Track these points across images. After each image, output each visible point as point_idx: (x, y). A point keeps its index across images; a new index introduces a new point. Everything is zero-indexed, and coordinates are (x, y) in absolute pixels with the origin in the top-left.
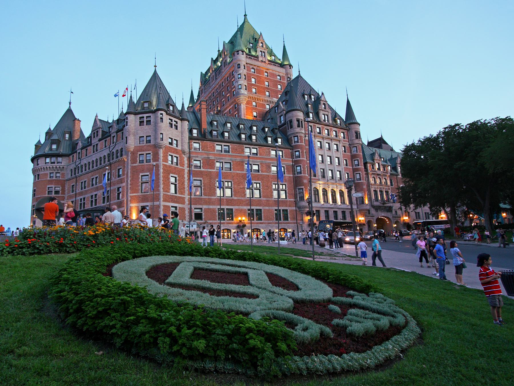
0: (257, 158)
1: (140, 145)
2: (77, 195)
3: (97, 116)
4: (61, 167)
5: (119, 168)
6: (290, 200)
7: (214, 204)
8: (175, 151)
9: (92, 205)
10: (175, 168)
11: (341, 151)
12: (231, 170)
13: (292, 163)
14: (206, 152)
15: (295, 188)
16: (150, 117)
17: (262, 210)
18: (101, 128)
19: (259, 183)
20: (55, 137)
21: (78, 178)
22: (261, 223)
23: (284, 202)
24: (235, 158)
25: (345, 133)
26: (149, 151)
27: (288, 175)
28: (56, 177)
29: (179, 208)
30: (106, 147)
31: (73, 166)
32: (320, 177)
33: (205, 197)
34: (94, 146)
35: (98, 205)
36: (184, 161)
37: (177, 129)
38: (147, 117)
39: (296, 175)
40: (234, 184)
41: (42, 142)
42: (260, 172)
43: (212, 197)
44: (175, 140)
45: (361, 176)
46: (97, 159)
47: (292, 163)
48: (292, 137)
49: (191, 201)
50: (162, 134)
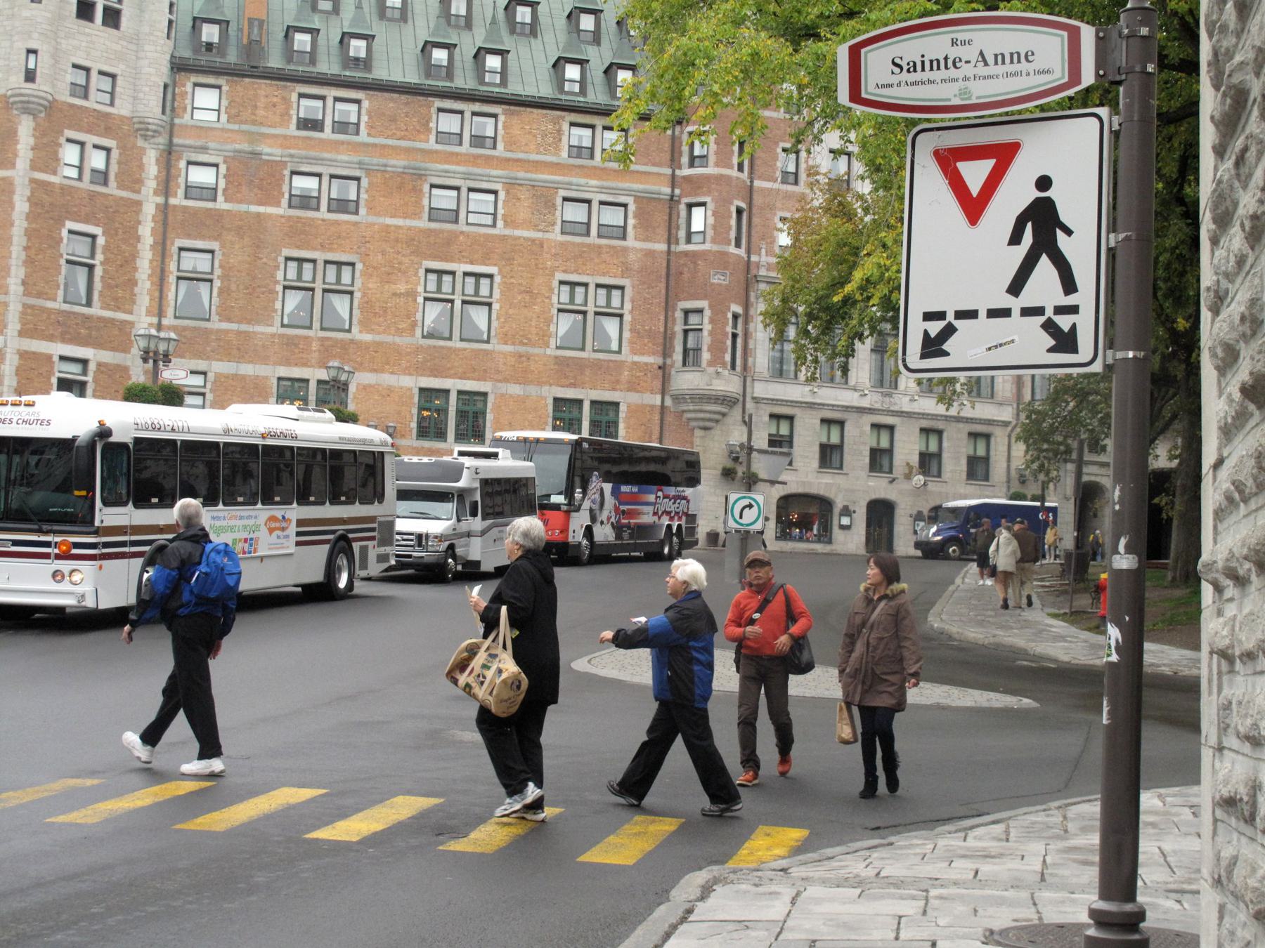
6: (636, 358)
7: (264, 360)
8: (103, 123)
10: (93, 196)
12: (357, 213)
14: (245, 127)
15: (668, 307)
17: (491, 399)
19: (491, 276)
23: (606, 371)
24: (382, 156)
27: (639, 245)
29: (99, 365)
33: (225, 326)
36: (141, 167)
39: (682, 247)
42: (500, 223)
43: (259, 329)
44: (101, 73)
47: (668, 190)
50: (35, 52)
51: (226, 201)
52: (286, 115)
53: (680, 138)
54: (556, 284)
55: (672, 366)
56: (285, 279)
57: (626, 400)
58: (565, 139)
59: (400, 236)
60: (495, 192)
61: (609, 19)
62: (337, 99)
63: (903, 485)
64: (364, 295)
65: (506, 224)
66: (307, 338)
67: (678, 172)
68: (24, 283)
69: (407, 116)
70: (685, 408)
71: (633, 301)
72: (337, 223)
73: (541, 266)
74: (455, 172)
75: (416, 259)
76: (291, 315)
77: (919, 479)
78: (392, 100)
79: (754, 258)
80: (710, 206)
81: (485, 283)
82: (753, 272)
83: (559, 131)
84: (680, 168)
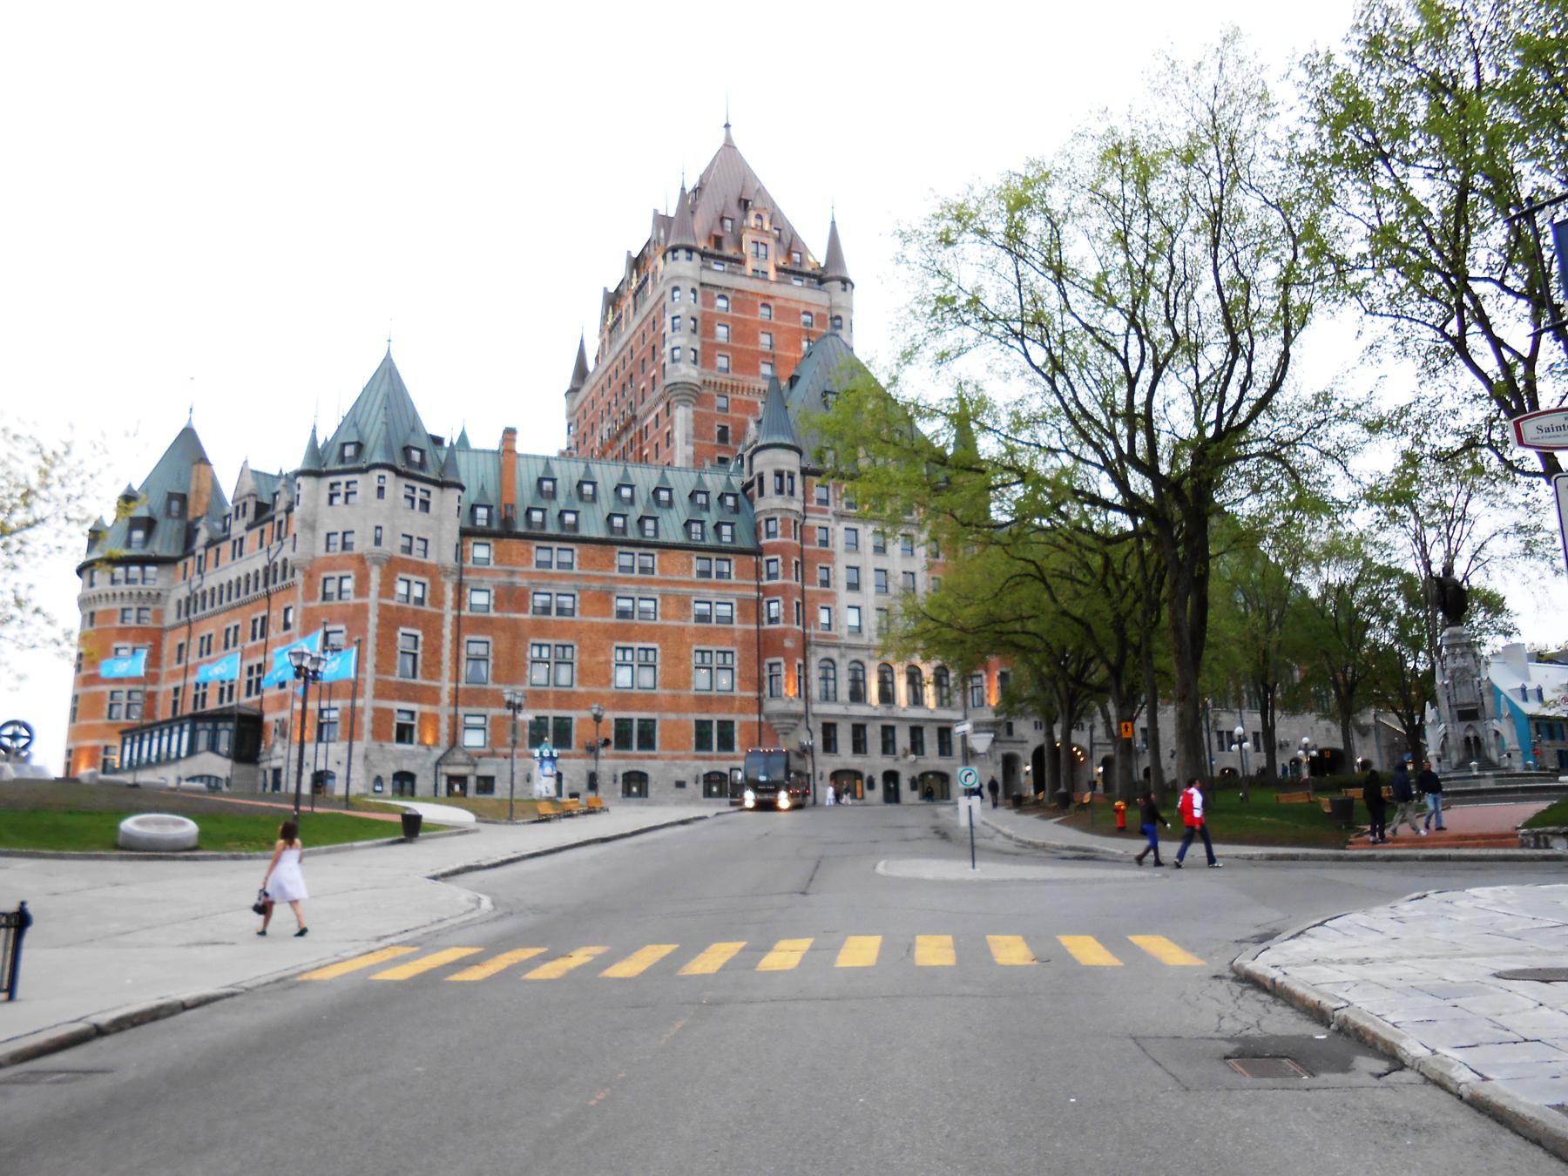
0: (651, 582)
1: (329, 554)
2: (190, 672)
3: (246, 462)
4: (154, 593)
5: (286, 605)
8: (421, 569)
9: (221, 700)
10: (415, 612)
15: (760, 662)
16: (355, 482)
18: (254, 495)
19: (654, 650)
20: (140, 511)
21: (194, 626)
22: (651, 757)
23: (725, 701)
26: (347, 568)
28: (139, 619)
30: (261, 546)
31: (182, 592)
32: (845, 631)
34: (235, 542)
35: (234, 702)
36: (443, 593)
37: (427, 510)
38: (348, 484)
39: (767, 626)
40: (581, 651)
41: (109, 521)
42: (658, 618)
44: (419, 539)
46: (239, 579)
47: (755, 594)
49: (457, 697)
52: (529, 560)
57: (738, 719)
60: (655, 600)
63: (903, 761)
64: (580, 663)
65: (664, 616)
68: (376, 666)
72: (562, 622)
74: (632, 590)
77: (912, 757)
81: (651, 653)
83: (691, 563)
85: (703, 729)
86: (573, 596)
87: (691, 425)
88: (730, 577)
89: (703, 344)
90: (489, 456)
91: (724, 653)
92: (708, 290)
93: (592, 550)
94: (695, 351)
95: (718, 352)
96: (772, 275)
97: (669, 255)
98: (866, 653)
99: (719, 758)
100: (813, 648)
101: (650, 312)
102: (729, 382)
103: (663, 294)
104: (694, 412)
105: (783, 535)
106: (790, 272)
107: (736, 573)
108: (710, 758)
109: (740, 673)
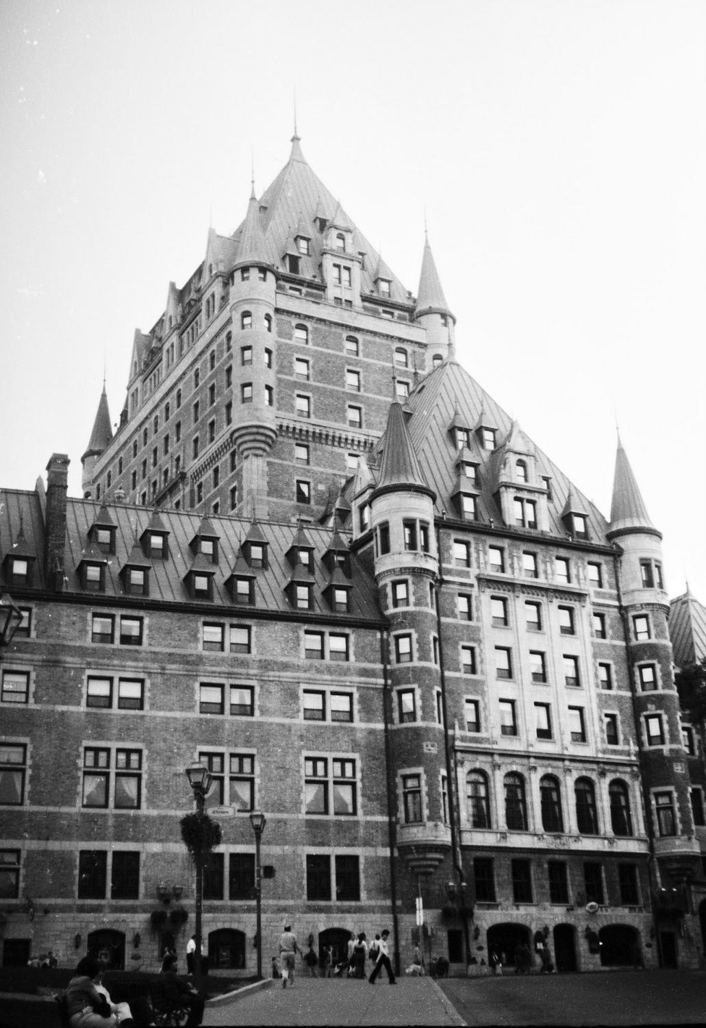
6: (369, 818)
7: (68, 836)
11: (587, 630)
12: (141, 708)
13: (381, 681)
23: (346, 832)
25: (604, 568)
27: (363, 725)
32: (497, 732)
33: (35, 808)
39: (397, 725)
40: (152, 759)
42: (257, 712)
43: (64, 809)
45: (666, 727)
47: (381, 681)
48: (386, 585)
51: (36, 702)
52: (83, 631)
53: (387, 640)
54: (302, 760)
55: (397, 822)
56: (85, 766)
58: (302, 643)
59: (178, 726)
60: (252, 688)
61: (318, 556)
62: (124, 617)
63: (580, 911)
64: (150, 776)
65: (262, 713)
66: (105, 815)
67: (389, 667)
69: (179, 629)
70: (411, 857)
71: (362, 771)
73: (290, 746)
75: (191, 745)
76: (88, 797)
78: (167, 617)
79: (450, 732)
80: (418, 692)
82: (450, 743)
83: (298, 639)
84: (389, 663)
85: (317, 865)
86: (142, 681)
87: (267, 479)
88: (347, 659)
89: (280, 380)
90: (23, 498)
91: (343, 761)
92: (284, 317)
93: (166, 620)
94: (269, 388)
95: (298, 392)
96: (358, 302)
97: (238, 275)
98: (525, 761)
99: (342, 910)
100: (459, 755)
101: (208, 346)
102: (311, 429)
103: (229, 321)
104: (269, 464)
105: (416, 605)
106: (376, 303)
107: (355, 654)
108: (327, 910)
109: (364, 787)
